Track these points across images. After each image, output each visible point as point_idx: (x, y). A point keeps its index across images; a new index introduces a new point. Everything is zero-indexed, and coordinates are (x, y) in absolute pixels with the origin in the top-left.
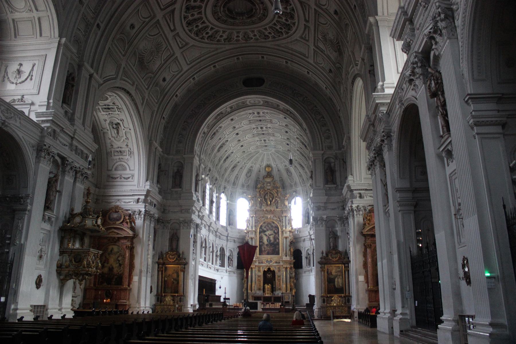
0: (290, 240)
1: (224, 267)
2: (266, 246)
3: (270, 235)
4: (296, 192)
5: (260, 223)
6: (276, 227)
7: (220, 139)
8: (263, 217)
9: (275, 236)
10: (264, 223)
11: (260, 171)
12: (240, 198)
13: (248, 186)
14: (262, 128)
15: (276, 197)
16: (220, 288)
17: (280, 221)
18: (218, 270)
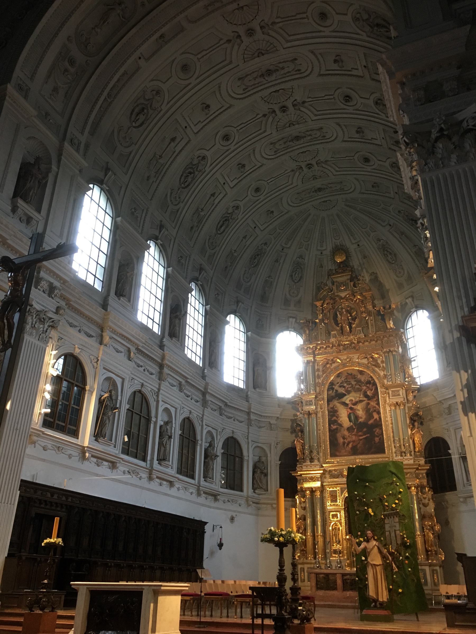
0: (410, 408)
1: (241, 490)
2: (346, 433)
3: (355, 404)
4: (412, 297)
5: (328, 377)
6: (369, 382)
7: (173, 140)
8: (334, 362)
9: (368, 404)
10: (338, 376)
11: (322, 266)
12: (282, 331)
13: (299, 302)
14: (284, 109)
15: (362, 313)
16: (221, 545)
17: (377, 365)
18: (215, 496)
